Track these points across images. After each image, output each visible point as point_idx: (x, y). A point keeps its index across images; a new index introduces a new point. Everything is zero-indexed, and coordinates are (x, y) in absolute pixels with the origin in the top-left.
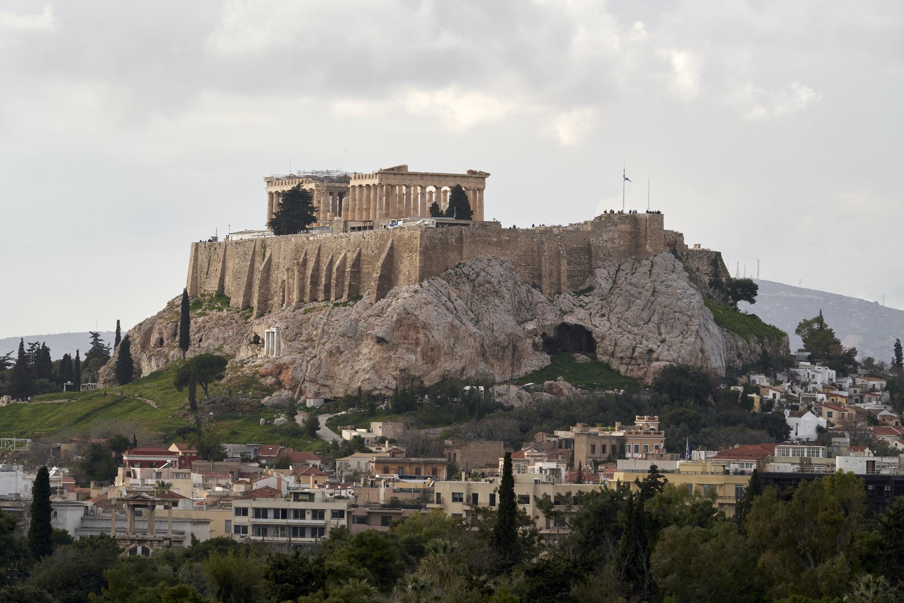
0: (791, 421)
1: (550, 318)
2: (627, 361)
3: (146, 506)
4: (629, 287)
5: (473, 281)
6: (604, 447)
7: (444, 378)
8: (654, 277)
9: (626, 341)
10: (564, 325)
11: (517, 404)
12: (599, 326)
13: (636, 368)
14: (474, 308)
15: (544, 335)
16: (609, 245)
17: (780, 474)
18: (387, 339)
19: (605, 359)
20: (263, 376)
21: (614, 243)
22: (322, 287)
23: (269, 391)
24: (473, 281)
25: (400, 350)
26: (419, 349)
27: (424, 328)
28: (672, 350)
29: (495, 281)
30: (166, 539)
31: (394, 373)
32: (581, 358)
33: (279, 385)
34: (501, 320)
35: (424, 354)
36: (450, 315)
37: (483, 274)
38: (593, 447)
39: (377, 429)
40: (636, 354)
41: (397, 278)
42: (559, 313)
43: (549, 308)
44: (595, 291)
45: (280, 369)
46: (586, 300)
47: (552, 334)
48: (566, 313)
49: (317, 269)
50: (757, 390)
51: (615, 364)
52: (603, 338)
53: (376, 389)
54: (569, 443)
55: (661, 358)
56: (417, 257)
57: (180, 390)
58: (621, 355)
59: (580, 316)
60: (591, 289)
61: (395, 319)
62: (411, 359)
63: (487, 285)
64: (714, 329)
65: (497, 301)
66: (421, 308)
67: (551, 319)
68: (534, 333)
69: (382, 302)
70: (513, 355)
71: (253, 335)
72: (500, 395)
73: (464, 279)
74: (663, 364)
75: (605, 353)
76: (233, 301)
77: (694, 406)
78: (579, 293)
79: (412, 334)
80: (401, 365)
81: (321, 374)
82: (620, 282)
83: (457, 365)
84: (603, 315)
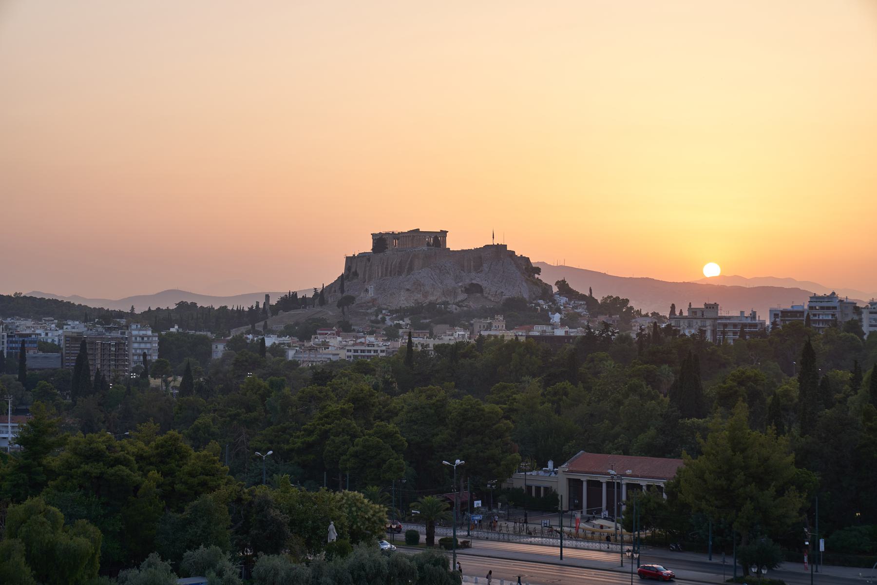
7: (430, 303)
12: (484, 284)
23: (370, 308)
28: (510, 293)
33: (374, 305)
39: (407, 321)
50: (539, 305)
51: (490, 297)
64: (524, 284)
67: (468, 281)
77: (516, 311)
83: (435, 298)
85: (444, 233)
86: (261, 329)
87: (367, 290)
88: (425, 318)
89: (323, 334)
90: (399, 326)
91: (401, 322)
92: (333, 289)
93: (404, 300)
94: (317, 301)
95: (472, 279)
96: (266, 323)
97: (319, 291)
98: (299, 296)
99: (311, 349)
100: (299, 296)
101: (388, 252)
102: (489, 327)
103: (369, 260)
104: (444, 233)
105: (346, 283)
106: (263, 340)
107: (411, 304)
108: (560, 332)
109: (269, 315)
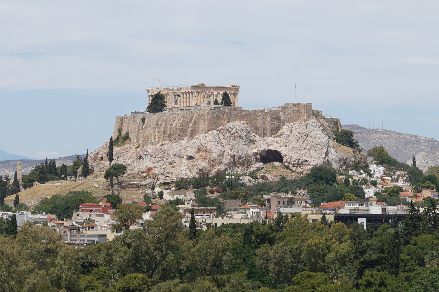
0: (366, 191)
1: (263, 147)
2: (296, 165)
3: (76, 229)
4: (297, 134)
5: (230, 132)
6: (284, 202)
8: (308, 130)
9: (295, 157)
10: (269, 150)
11: (248, 184)
12: (283, 151)
13: (300, 168)
14: (230, 143)
15: (260, 155)
16: (289, 116)
17: (344, 214)
18: (194, 157)
19: (287, 164)
20: (142, 173)
21: (291, 115)
22: (168, 135)
24: (230, 132)
25: (199, 161)
26: (207, 161)
27: (209, 152)
28: (315, 159)
29: (239, 132)
30: (84, 243)
31: (197, 171)
32: (277, 164)
34: (241, 148)
35: (209, 163)
36: (220, 146)
37: (234, 129)
38: (279, 202)
40: (300, 162)
41: (198, 130)
42: (267, 145)
43: (262, 143)
44: (283, 136)
45: (150, 169)
46: (279, 139)
47: (264, 154)
48: (270, 145)
49: (165, 128)
50: (351, 177)
51: (291, 166)
52: (286, 156)
53: (189, 178)
54: (269, 201)
55: (310, 164)
56: (206, 122)
57: (107, 179)
58: (294, 163)
59: (276, 147)
60: (281, 134)
61: (197, 148)
62: (205, 165)
63: (236, 134)
65: (240, 140)
66: (208, 143)
68: (256, 154)
69: (192, 141)
70: (248, 163)
71: (139, 155)
72: (241, 180)
73: (227, 131)
74: (312, 166)
75: (287, 162)
76: (132, 141)
78: (276, 137)
79: (204, 154)
80: (200, 167)
81: (166, 172)
82: (293, 132)
84: (286, 146)
85: (236, 88)
86: (12, 204)
87: (140, 158)
88: (212, 192)
89: (86, 211)
90: (179, 202)
91: (181, 197)
92: (100, 156)
93: (185, 170)
94: (80, 170)
95: (269, 145)
96: (17, 197)
97: (82, 159)
98: (58, 165)
99: (72, 228)
100: (58, 165)
101: (166, 111)
102: (290, 203)
103: (143, 121)
104: (236, 88)
105: (116, 149)
106: (14, 218)
107: (193, 175)
108: (376, 210)
109: (21, 187)
